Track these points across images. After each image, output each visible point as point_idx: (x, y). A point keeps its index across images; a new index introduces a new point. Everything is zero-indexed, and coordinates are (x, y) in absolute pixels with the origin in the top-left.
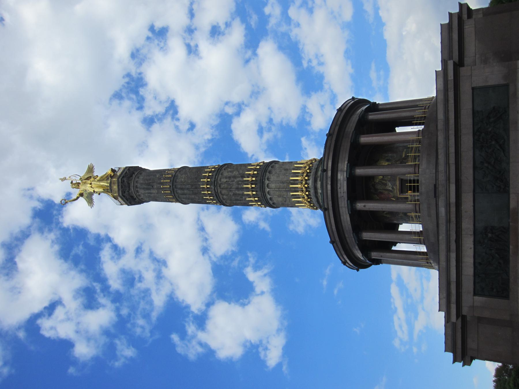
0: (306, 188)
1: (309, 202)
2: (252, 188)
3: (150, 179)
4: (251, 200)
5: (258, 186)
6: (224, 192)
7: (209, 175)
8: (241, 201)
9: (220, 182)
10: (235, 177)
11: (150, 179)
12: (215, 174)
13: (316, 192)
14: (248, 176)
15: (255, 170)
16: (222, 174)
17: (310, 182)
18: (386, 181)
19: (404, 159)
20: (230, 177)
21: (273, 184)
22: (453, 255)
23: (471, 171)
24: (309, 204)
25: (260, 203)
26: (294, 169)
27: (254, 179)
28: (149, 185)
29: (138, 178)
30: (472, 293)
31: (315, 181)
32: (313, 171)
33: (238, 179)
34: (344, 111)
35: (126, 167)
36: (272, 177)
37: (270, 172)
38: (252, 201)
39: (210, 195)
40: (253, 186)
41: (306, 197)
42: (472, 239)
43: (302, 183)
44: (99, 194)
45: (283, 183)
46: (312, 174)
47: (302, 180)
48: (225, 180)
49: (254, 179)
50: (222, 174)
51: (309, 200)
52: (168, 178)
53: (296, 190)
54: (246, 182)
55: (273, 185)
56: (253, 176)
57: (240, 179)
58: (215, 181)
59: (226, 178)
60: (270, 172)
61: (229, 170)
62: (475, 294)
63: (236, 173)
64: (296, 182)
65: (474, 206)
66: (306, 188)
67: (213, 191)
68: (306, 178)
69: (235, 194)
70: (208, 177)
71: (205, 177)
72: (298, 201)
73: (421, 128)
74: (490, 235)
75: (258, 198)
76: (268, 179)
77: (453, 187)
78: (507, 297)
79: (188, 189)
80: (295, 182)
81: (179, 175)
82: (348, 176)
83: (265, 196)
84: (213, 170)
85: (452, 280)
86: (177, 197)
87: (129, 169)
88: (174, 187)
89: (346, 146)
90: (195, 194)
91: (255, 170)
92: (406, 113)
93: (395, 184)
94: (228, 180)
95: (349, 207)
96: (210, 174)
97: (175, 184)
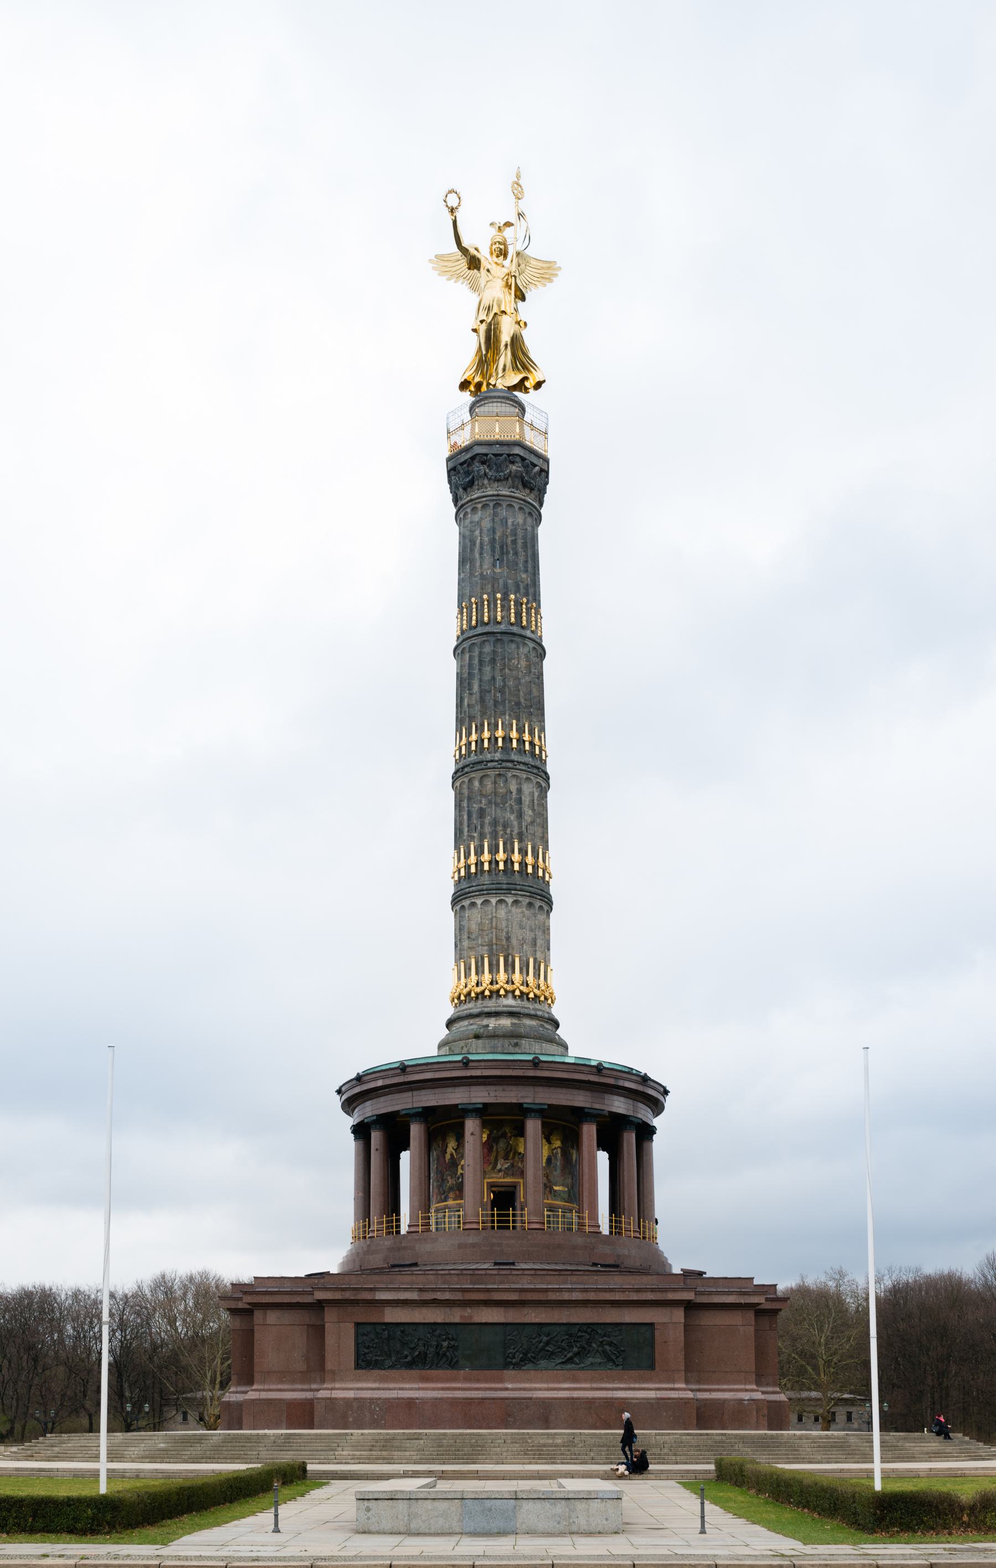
0: (498, 991)
1: (469, 994)
2: (497, 862)
3: (516, 554)
4: (469, 854)
5: (502, 878)
6: (489, 785)
7: (524, 741)
8: (468, 826)
9: (510, 774)
10: (520, 816)
11: (516, 554)
12: (528, 759)
13: (489, 1015)
14: (523, 852)
15: (535, 867)
16: (528, 779)
17: (510, 1001)
18: (513, 1158)
19: (551, 1189)
20: (519, 801)
21: (508, 914)
22: (414, 1296)
23: (537, 1320)
24: (465, 991)
25: (463, 873)
26: (535, 960)
27: (516, 867)
28: (502, 547)
29: (521, 508)
30: (359, 1321)
31: (511, 1014)
32: (530, 1007)
33: (515, 823)
34: (640, 1088)
35: (547, 461)
36: (520, 910)
37: (530, 905)
38: (467, 856)
39: (480, 742)
40: (501, 866)
41: (479, 989)
42: (439, 1321)
43: (507, 983)
44: (475, 330)
45: (508, 938)
46: (526, 1004)
47: (513, 983)
48: (513, 787)
49: (516, 867)
50: (528, 779)
51: (473, 995)
52: (518, 615)
53: (494, 968)
54: (509, 847)
55: (502, 912)
56: (523, 865)
57: (516, 831)
58: (512, 761)
59: (519, 791)
60: (530, 905)
61: (536, 794)
62: (357, 1325)
63: (528, 813)
64: (510, 969)
65: (486, 1324)
66: (498, 991)
67: (489, 757)
68: (517, 993)
69: (482, 813)
70: (521, 741)
71: (521, 731)
72: (470, 969)
73: (605, 1229)
74: (445, 1344)
75: (476, 873)
76: (516, 902)
77: (514, 1297)
78: (358, 1366)
79: (494, 678)
80: (510, 967)
81: (526, 650)
82: (525, 1106)
83: (481, 892)
84: (537, 752)
85: (377, 1293)
86: (474, 640)
87: (542, 470)
88: (499, 637)
89: (580, 1099)
90: (482, 700)
91: (535, 867)
92: (632, 1195)
93: (506, 1174)
94: (514, 795)
95: (472, 1107)
96: (527, 747)
97: (506, 638)
